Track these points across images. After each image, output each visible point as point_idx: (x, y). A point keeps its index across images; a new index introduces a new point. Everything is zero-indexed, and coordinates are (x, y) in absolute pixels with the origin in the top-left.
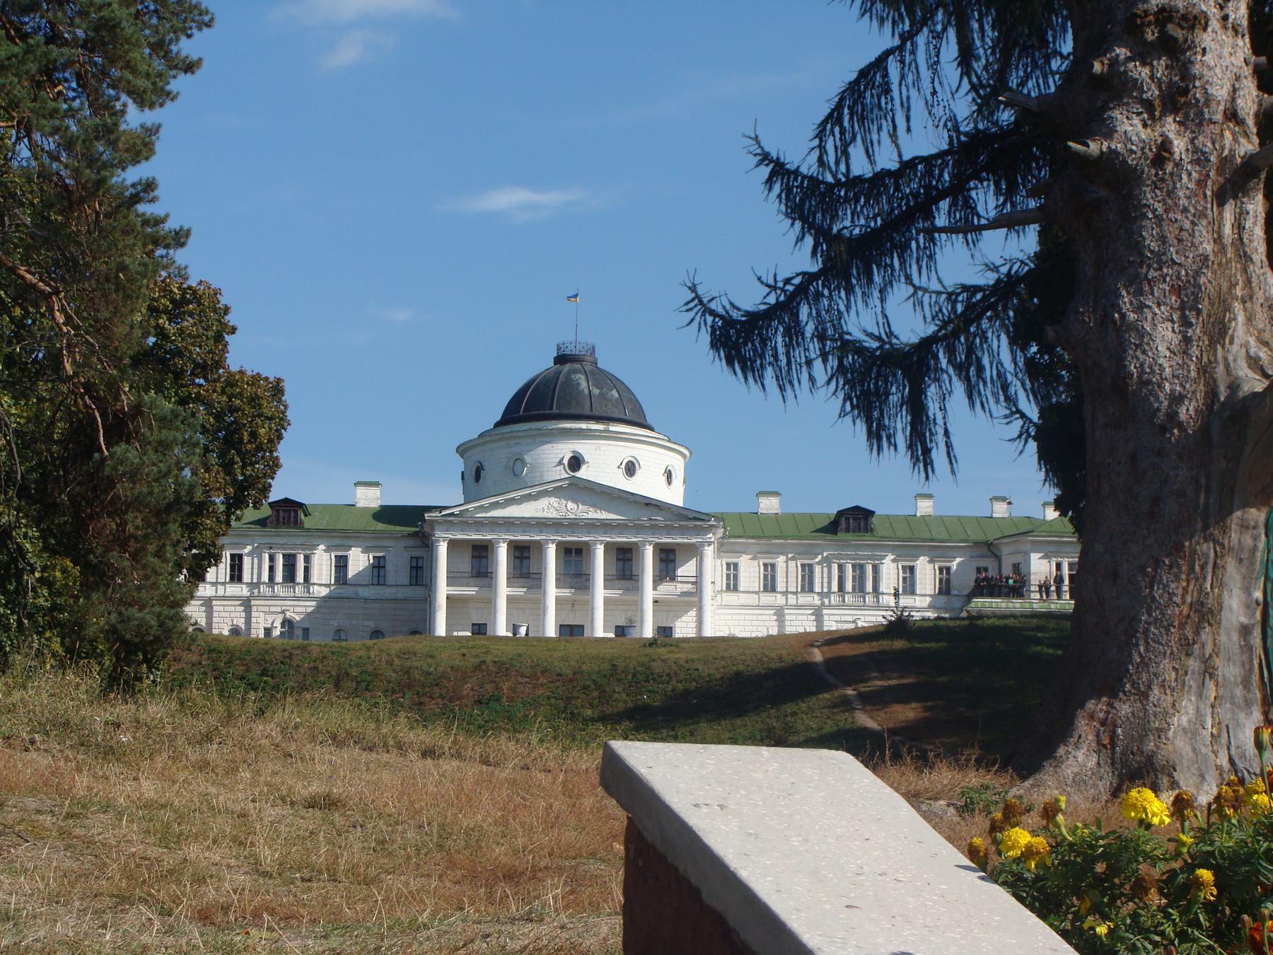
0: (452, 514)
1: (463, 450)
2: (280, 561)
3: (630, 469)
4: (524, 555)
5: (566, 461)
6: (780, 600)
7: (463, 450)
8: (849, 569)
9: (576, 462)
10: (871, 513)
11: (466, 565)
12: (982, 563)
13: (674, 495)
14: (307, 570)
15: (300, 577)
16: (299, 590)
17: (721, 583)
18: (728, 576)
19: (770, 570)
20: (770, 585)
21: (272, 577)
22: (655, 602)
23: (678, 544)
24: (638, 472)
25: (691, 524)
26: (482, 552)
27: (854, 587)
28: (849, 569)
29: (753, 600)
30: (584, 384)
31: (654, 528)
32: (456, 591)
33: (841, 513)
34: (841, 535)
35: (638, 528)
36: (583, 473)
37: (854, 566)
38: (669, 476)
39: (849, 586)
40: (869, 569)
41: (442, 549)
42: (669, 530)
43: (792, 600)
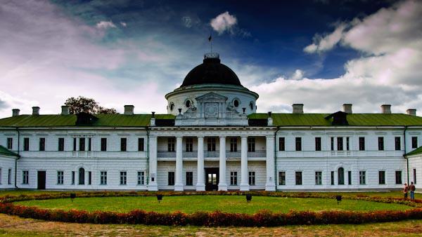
1: (168, 97)
7: (168, 97)
15: (87, 148)
16: (85, 155)
37: (338, 138)
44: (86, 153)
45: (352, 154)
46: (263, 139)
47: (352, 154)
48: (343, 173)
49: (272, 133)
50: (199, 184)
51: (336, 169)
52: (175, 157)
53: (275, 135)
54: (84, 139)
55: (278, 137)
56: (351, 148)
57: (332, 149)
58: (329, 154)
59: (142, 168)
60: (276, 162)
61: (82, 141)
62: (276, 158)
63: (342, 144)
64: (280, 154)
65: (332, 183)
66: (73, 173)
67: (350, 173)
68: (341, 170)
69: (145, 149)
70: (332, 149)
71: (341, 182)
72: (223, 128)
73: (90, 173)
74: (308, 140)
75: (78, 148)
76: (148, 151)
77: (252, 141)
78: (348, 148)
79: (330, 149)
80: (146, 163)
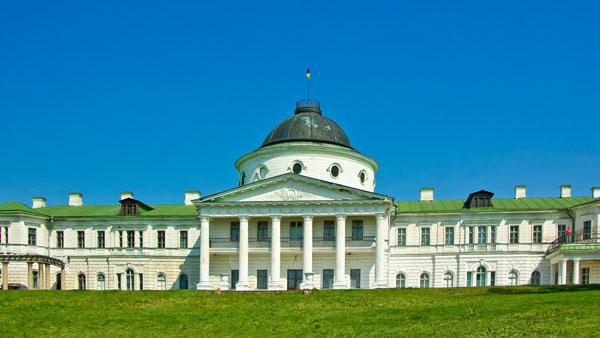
0: (210, 201)
2: (125, 234)
3: (335, 171)
4: (262, 227)
5: (292, 168)
6: (432, 250)
8: (476, 230)
9: (298, 167)
10: (491, 195)
11: (226, 233)
12: (563, 222)
13: (369, 186)
14: (141, 239)
17: (394, 240)
18: (399, 236)
19: (426, 232)
20: (426, 241)
21: (121, 244)
22: (348, 254)
23: (365, 217)
24: (340, 175)
25: (371, 202)
26: (235, 225)
27: (479, 241)
28: (476, 230)
29: (416, 251)
30: (308, 122)
31: (345, 205)
32: (215, 250)
33: (472, 196)
34: (471, 209)
35: (334, 205)
36: (303, 173)
37: (480, 228)
38: (362, 177)
39: (476, 240)
40: (489, 229)
41: (205, 225)
42: (356, 206)
43: (440, 250)
44: (136, 252)
45: (498, 248)
47: (498, 248)
48: (484, 276)
51: (474, 267)
54: (133, 232)
56: (498, 240)
57: (471, 241)
58: (467, 249)
61: (131, 234)
63: (485, 236)
66: (119, 275)
67: (493, 274)
70: (471, 241)
73: (141, 275)
74: (437, 231)
75: (125, 245)
78: (493, 241)
79: (467, 241)
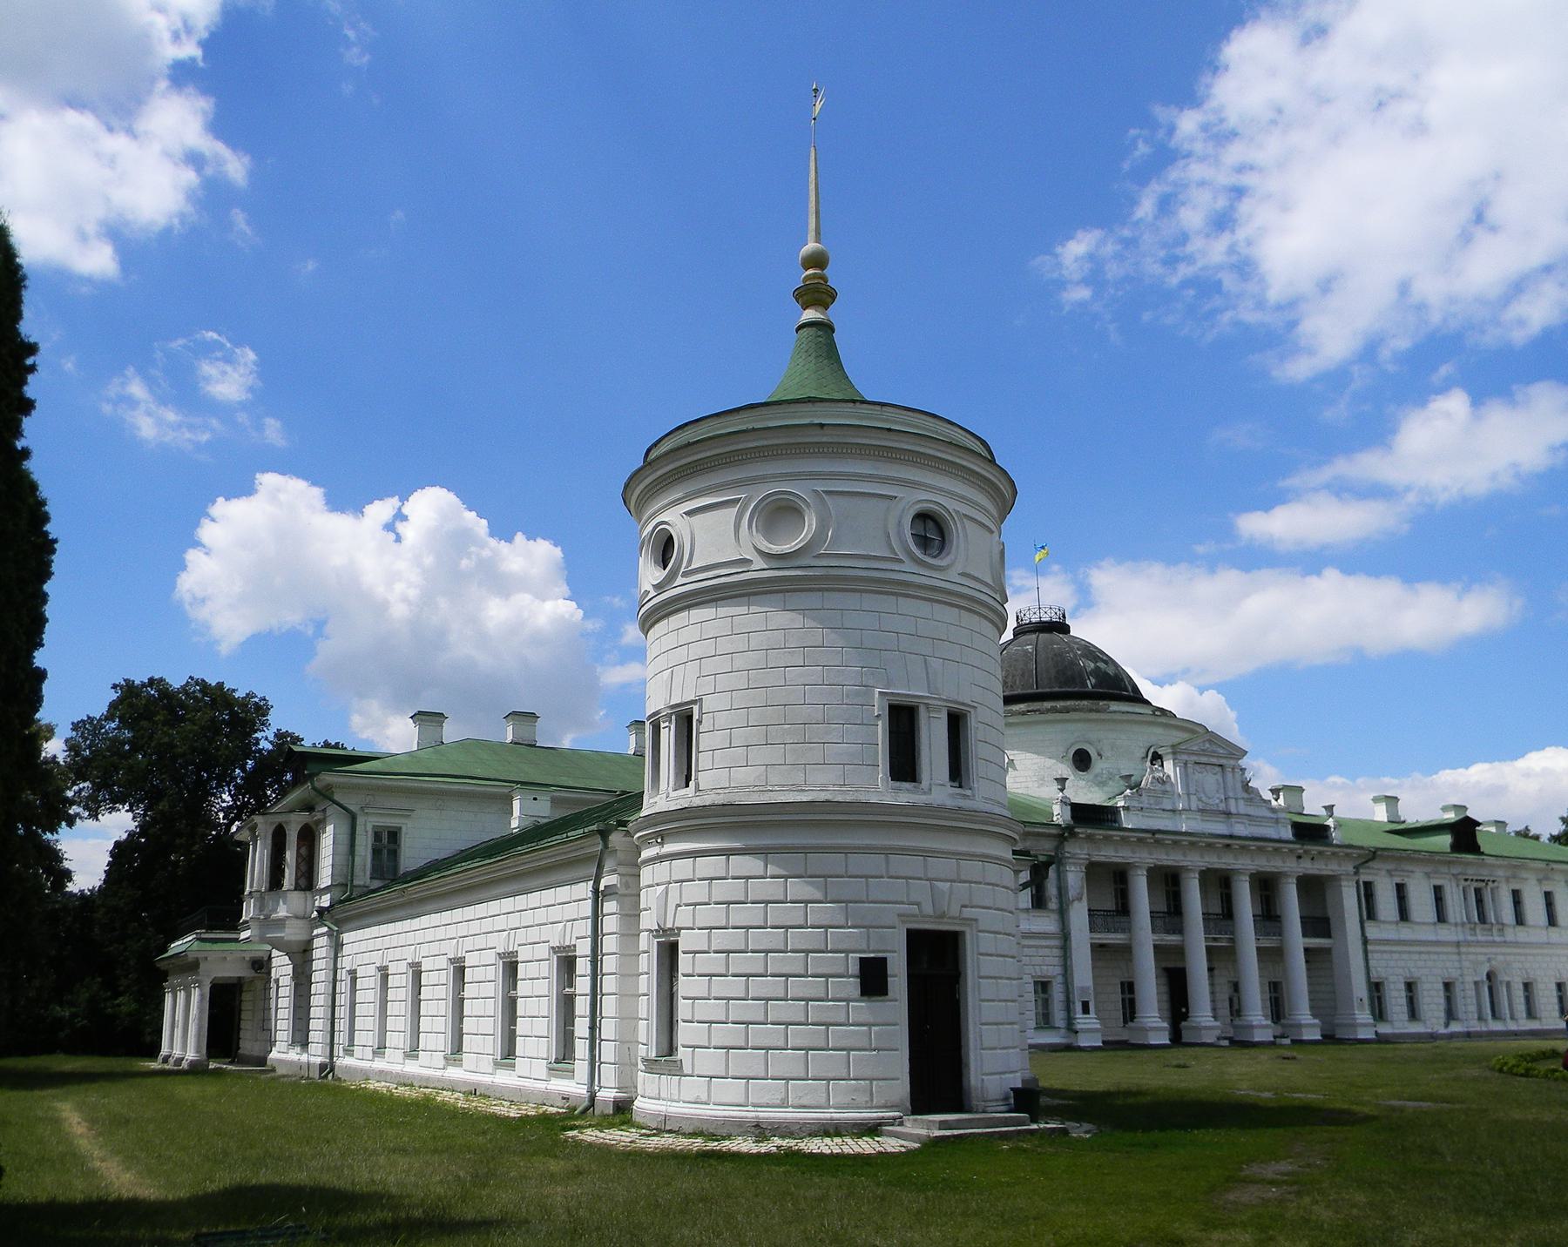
46: (1334, 879)
49: (1349, 867)
50: (1153, 1020)
52: (1127, 929)
53: (1356, 873)
55: (1364, 878)
59: (1050, 968)
60: (1366, 952)
62: (1365, 941)
64: (1373, 931)
65: (1480, 1018)
68: (1489, 976)
69: (1053, 904)
71: (1495, 1015)
72: (1253, 845)
76: (1063, 913)
77: (1313, 887)
80: (1056, 952)
